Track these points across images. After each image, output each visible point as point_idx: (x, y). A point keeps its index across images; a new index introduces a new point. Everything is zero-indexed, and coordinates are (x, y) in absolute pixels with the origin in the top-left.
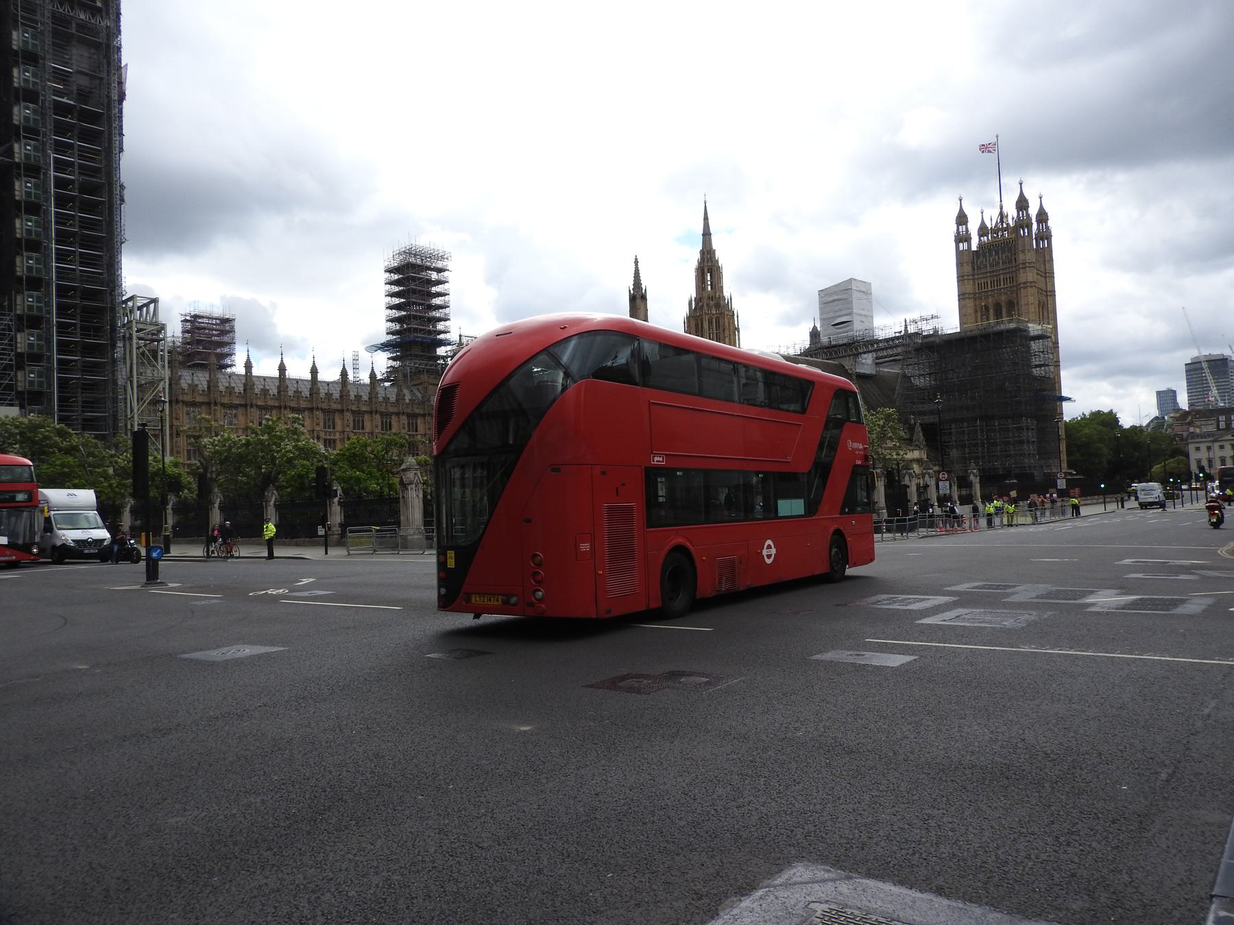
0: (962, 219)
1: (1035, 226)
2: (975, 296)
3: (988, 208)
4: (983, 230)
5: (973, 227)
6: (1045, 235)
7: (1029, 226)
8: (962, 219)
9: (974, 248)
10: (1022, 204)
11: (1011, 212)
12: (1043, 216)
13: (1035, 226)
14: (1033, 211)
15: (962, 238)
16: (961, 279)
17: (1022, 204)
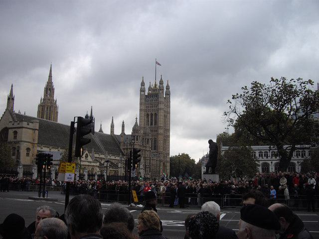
0: (143, 84)
1: (165, 90)
2: (146, 111)
3: (150, 82)
4: (150, 89)
5: (147, 87)
6: (168, 94)
7: (163, 90)
8: (143, 84)
9: (146, 94)
10: (161, 82)
11: (158, 84)
12: (168, 88)
13: (165, 90)
14: (165, 85)
15: (142, 90)
16: (141, 104)
17: (161, 82)
